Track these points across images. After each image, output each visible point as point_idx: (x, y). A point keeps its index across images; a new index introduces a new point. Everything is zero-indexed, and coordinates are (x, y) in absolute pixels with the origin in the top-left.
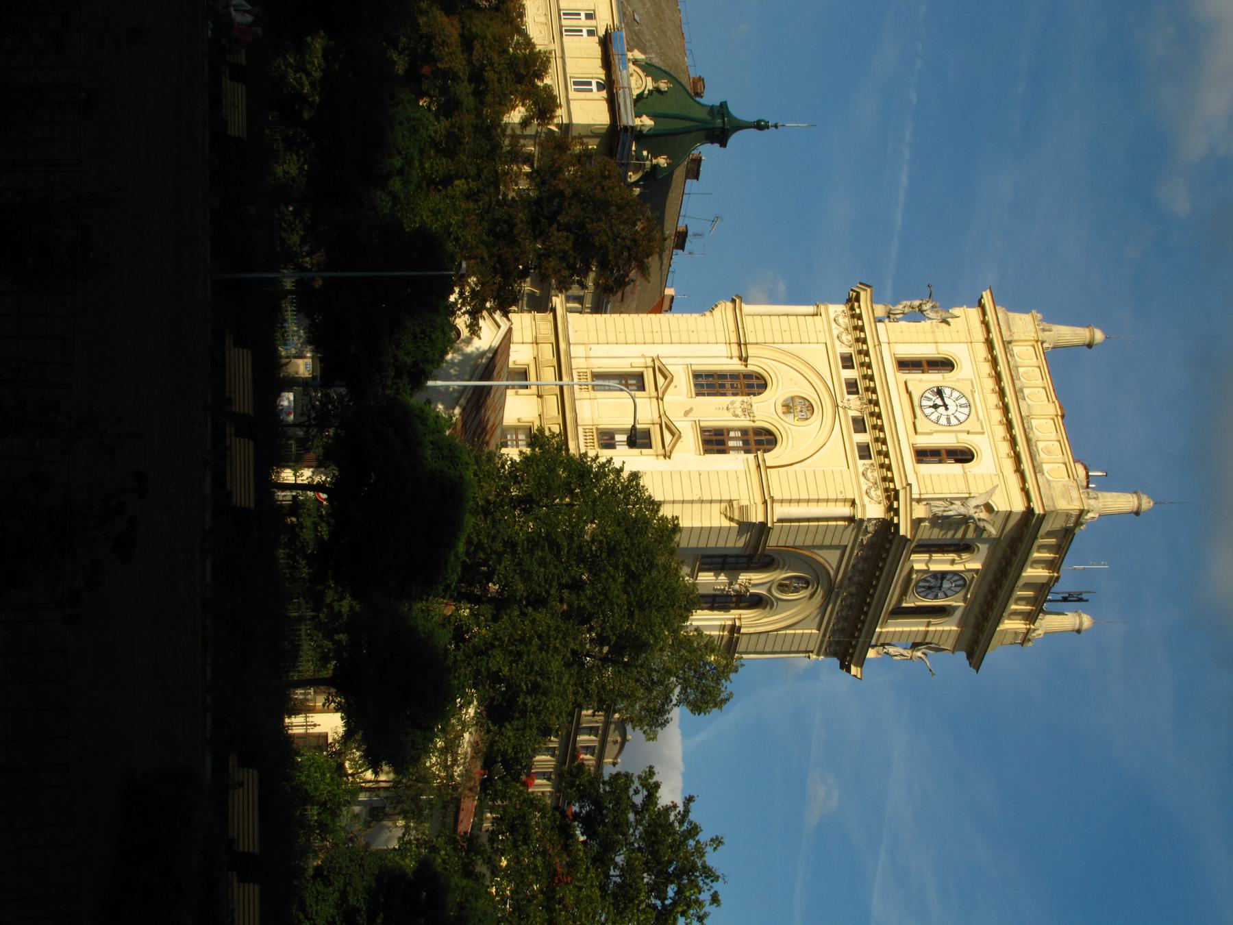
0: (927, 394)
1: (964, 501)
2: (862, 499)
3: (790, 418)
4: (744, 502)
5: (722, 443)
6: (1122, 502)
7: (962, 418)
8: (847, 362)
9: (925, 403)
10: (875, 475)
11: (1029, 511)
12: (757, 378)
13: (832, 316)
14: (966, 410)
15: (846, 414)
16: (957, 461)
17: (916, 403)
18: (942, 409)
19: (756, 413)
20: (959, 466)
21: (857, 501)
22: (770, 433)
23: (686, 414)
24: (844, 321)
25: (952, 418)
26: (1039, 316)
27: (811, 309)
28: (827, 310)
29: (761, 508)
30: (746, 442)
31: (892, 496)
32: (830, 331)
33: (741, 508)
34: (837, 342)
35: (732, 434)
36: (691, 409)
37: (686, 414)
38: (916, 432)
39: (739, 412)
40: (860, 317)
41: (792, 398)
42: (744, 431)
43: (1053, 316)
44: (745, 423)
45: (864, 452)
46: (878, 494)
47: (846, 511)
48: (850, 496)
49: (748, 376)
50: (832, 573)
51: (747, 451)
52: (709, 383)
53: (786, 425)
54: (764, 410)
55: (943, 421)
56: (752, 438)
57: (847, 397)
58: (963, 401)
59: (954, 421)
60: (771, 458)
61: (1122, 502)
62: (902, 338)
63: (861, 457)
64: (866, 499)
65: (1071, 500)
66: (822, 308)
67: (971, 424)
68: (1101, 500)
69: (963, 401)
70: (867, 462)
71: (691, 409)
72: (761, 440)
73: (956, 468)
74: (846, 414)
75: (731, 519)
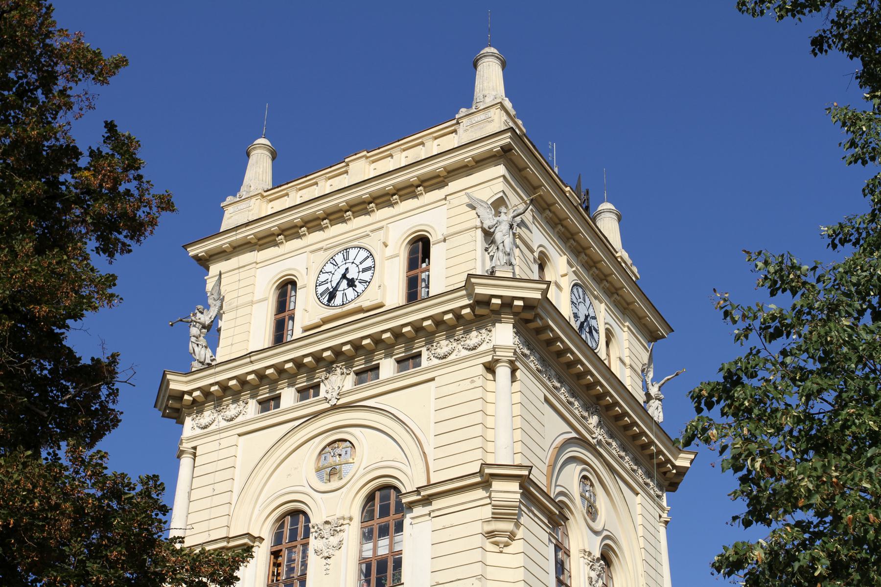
1: (488, 235)
2: (485, 353)
3: (348, 471)
4: (487, 512)
5: (382, 564)
6: (490, 78)
7: (363, 254)
8: (270, 403)
10: (444, 346)
11: (504, 155)
12: (282, 526)
13: (199, 431)
14: (353, 253)
15: (349, 393)
16: (426, 255)
17: (338, 311)
18: (349, 276)
19: (339, 515)
20: (434, 250)
21: (489, 358)
22: (370, 498)
24: (208, 415)
25: (361, 267)
26: (230, 199)
27: (186, 462)
28: (190, 439)
29: (496, 485)
30: (384, 531)
31: (483, 312)
32: (220, 431)
33: (496, 517)
35: (368, 554)
39: (334, 541)
40: (206, 392)
41: (318, 470)
42: (367, 536)
43: (232, 182)
44: (353, 532)
46: (474, 337)
47: (503, 371)
48: (481, 370)
49: (278, 538)
50: (574, 435)
51: (399, 527)
53: (361, 471)
54: (337, 507)
55: (366, 276)
56: (377, 522)
57: (322, 393)
58: (339, 258)
59: (369, 263)
60: (411, 480)
61: (490, 78)
62: (244, 332)
65: (489, 120)
66: (186, 446)
67: (373, 243)
68: (486, 93)
69: (339, 258)
72: (385, 507)
74: (349, 393)
75: (512, 536)
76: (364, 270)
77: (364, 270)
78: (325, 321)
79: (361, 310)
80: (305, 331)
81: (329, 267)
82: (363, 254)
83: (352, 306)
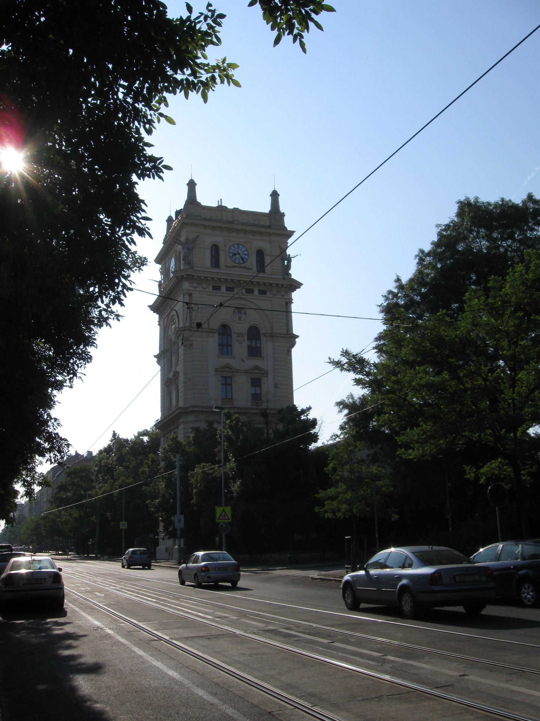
0: (233, 259)
7: (244, 249)
9: (237, 261)
23: (244, 361)
34: (207, 290)
36: (241, 359)
37: (244, 361)
38: (250, 269)
45: (262, 292)
52: (225, 348)
54: (240, 327)
59: (246, 252)
63: (266, 294)
64: (285, 297)
70: (268, 293)
71: (241, 359)
73: (267, 260)
76: (245, 254)
77: (245, 254)
78: (233, 267)
79: (245, 268)
80: (227, 266)
81: (232, 248)
82: (244, 249)
83: (242, 265)
